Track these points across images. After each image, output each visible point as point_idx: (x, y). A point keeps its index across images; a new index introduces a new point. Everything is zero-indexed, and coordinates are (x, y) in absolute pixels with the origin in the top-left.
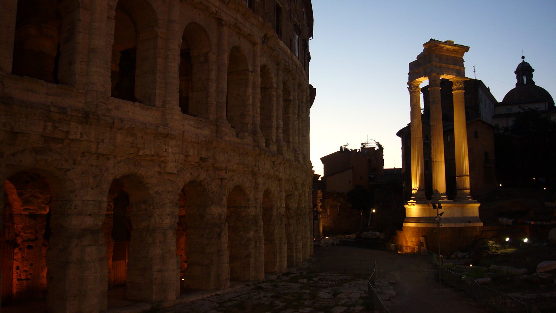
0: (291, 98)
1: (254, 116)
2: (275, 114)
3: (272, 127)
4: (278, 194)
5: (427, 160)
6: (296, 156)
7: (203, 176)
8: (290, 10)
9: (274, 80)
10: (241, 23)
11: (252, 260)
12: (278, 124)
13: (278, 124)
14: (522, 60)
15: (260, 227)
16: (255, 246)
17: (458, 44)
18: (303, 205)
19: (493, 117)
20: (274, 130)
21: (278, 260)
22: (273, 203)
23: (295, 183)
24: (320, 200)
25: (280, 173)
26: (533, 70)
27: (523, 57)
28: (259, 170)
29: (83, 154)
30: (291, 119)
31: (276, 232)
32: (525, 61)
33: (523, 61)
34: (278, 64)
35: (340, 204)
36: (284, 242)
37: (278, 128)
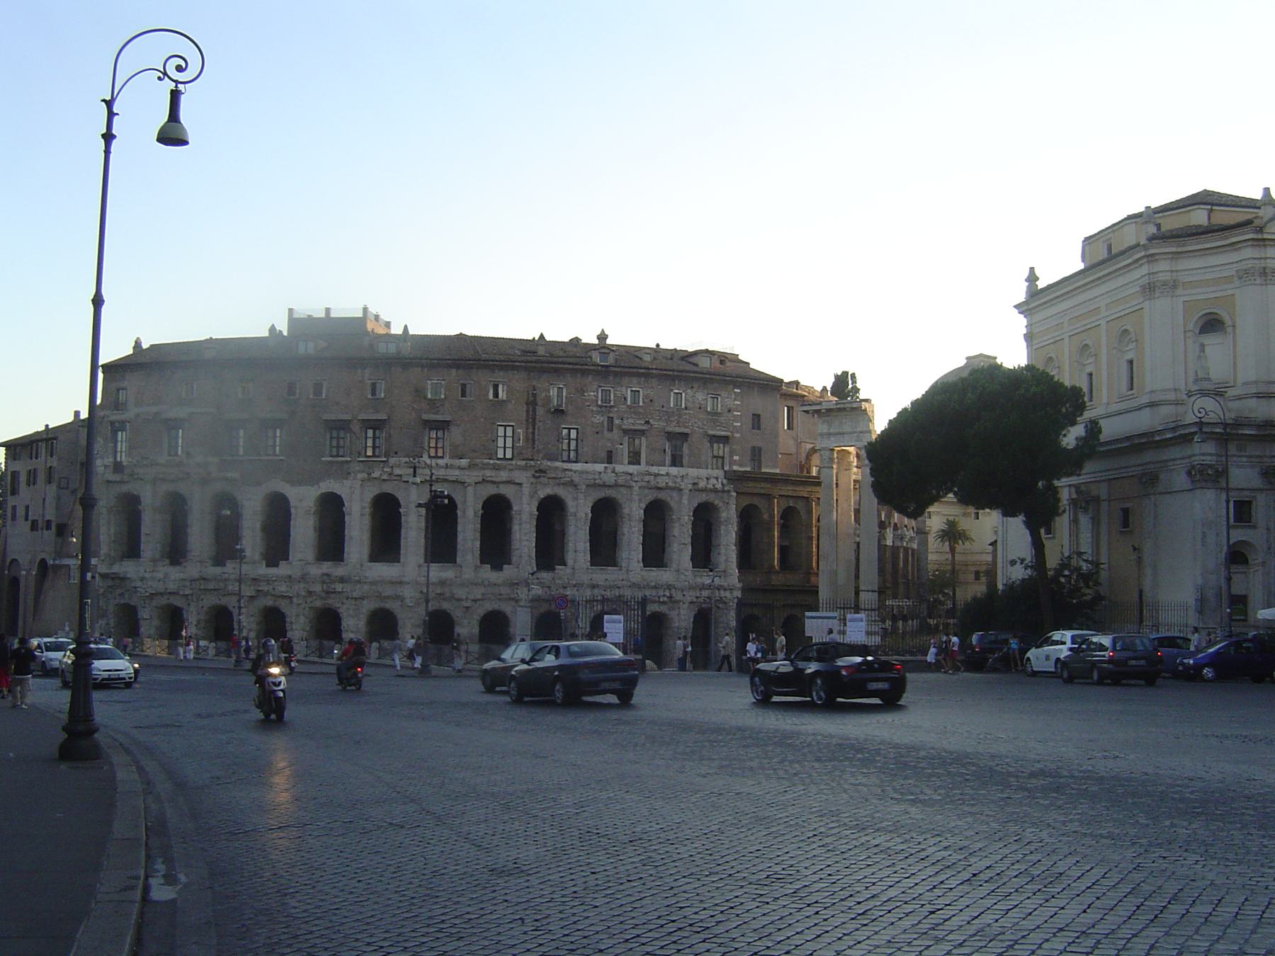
7: (446, 606)
8: (611, 420)
18: (677, 624)
29: (347, 599)
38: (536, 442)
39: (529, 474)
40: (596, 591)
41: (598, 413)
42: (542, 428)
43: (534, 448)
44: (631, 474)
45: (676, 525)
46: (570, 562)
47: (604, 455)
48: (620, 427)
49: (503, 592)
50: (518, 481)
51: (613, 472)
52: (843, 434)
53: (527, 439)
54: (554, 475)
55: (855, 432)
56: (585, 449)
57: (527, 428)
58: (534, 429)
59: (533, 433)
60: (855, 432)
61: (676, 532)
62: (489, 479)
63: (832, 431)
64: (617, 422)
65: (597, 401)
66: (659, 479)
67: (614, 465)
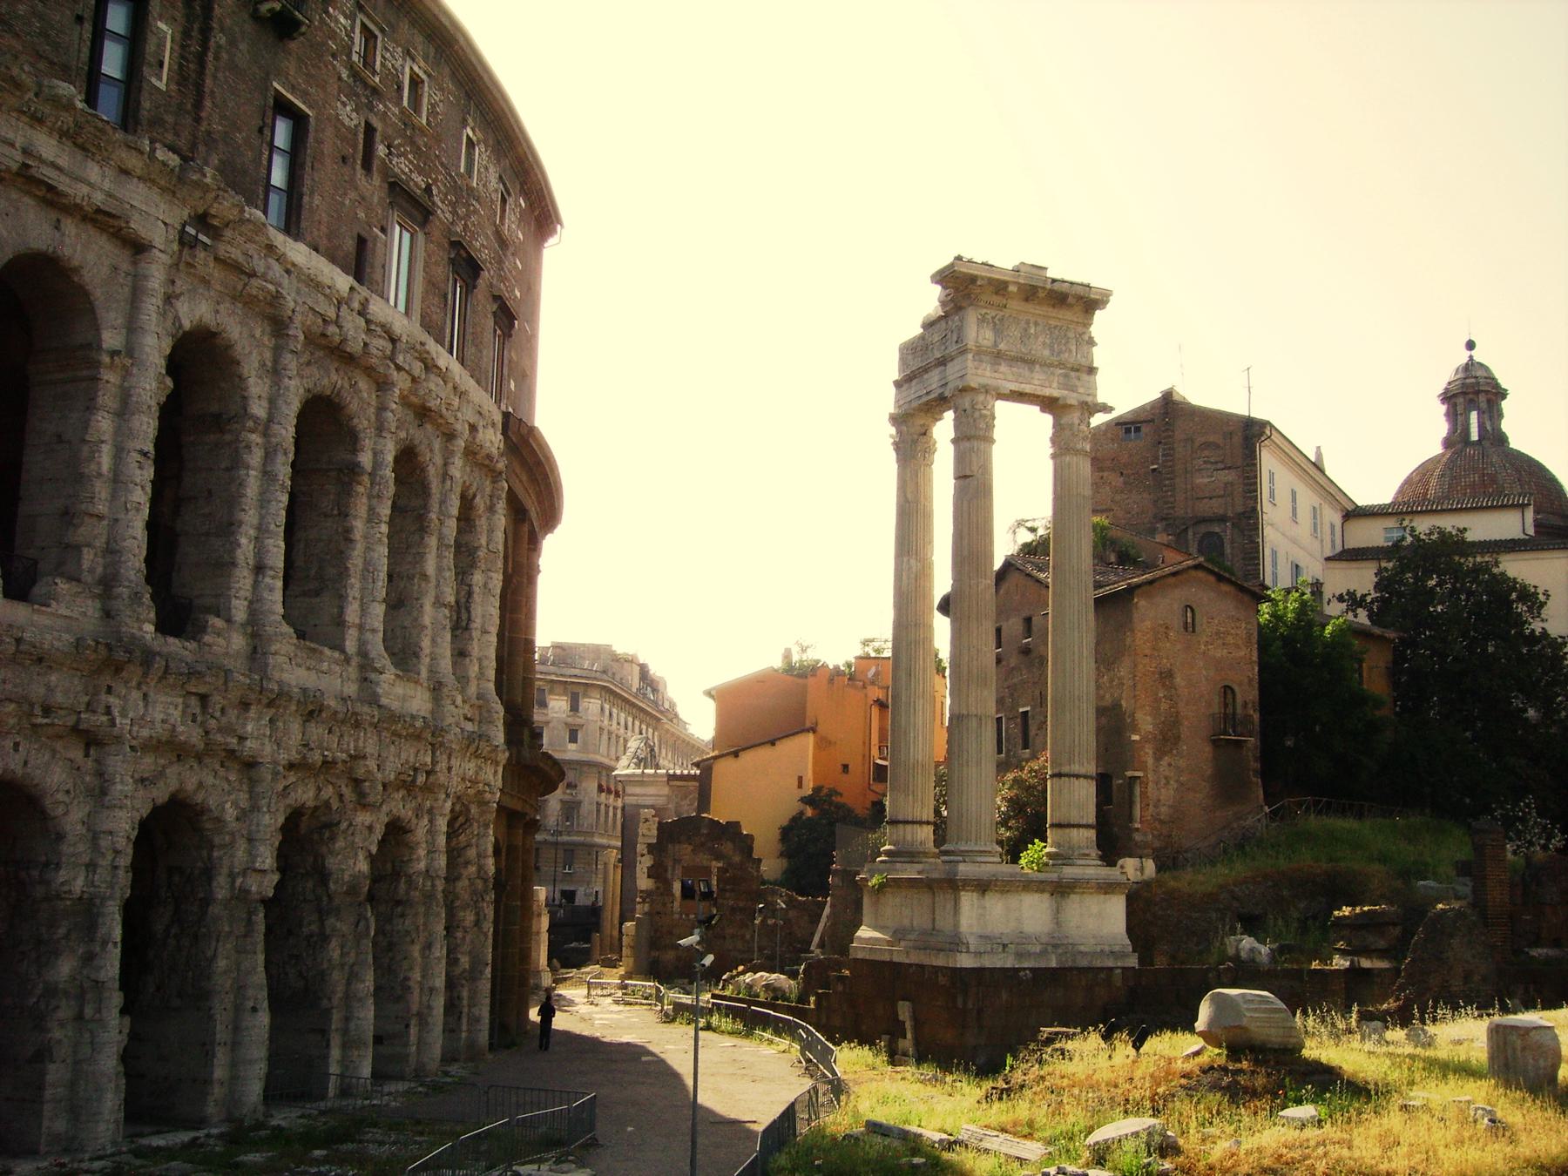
0: (365, 459)
1: (116, 520)
2: (250, 517)
3: (234, 564)
4: (238, 819)
5: (1028, 708)
6: (366, 679)
8: (370, 130)
9: (257, 387)
10: (54, 165)
11: (56, 1073)
12: (260, 551)
13: (260, 551)
14: (1469, 353)
15: (104, 943)
16: (79, 1017)
17: (1066, 279)
18: (422, 865)
19: (1328, 559)
20: (243, 580)
21: (219, 1073)
22: (216, 854)
23: (357, 783)
24: (649, 845)
25: (242, 739)
26: (1502, 394)
27: (1470, 345)
28: (113, 723)
30: (357, 535)
31: (222, 964)
32: (1477, 359)
33: (1471, 357)
34: (279, 326)
35: (720, 865)
36: (251, 1004)
37: (259, 569)
38: (208, 103)
39: (176, 214)
40: (317, 731)
41: (351, 94)
42: (225, 56)
43: (198, 120)
44: (394, 341)
45: (432, 541)
46: (240, 611)
47: (350, 245)
48: (386, 171)
49: (59, 698)
50: (137, 225)
51: (362, 313)
52: (1028, 362)
53: (180, 76)
54: (236, 254)
55: (1061, 365)
56: (317, 200)
57: (186, 34)
58: (205, 44)
59: (202, 64)
60: (1061, 365)
61: (430, 566)
62: (48, 174)
63: (1002, 346)
64: (381, 150)
65: (349, 55)
66: (434, 383)
67: (363, 291)
